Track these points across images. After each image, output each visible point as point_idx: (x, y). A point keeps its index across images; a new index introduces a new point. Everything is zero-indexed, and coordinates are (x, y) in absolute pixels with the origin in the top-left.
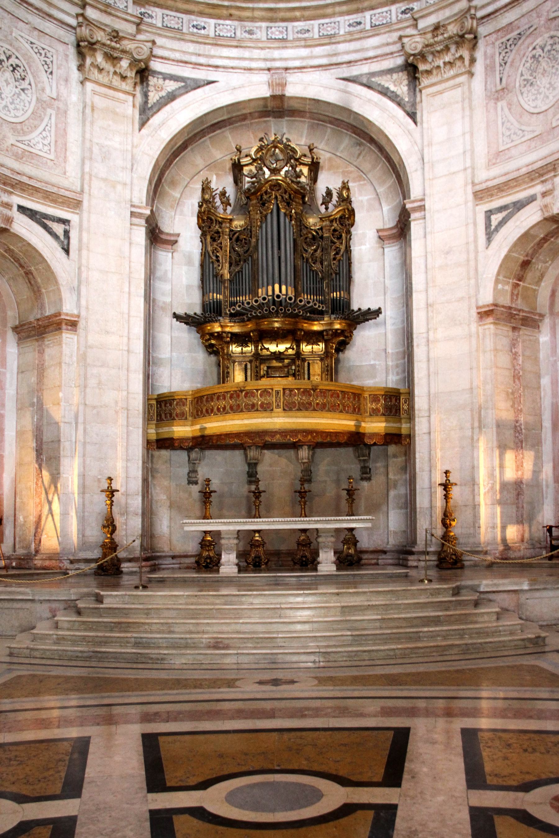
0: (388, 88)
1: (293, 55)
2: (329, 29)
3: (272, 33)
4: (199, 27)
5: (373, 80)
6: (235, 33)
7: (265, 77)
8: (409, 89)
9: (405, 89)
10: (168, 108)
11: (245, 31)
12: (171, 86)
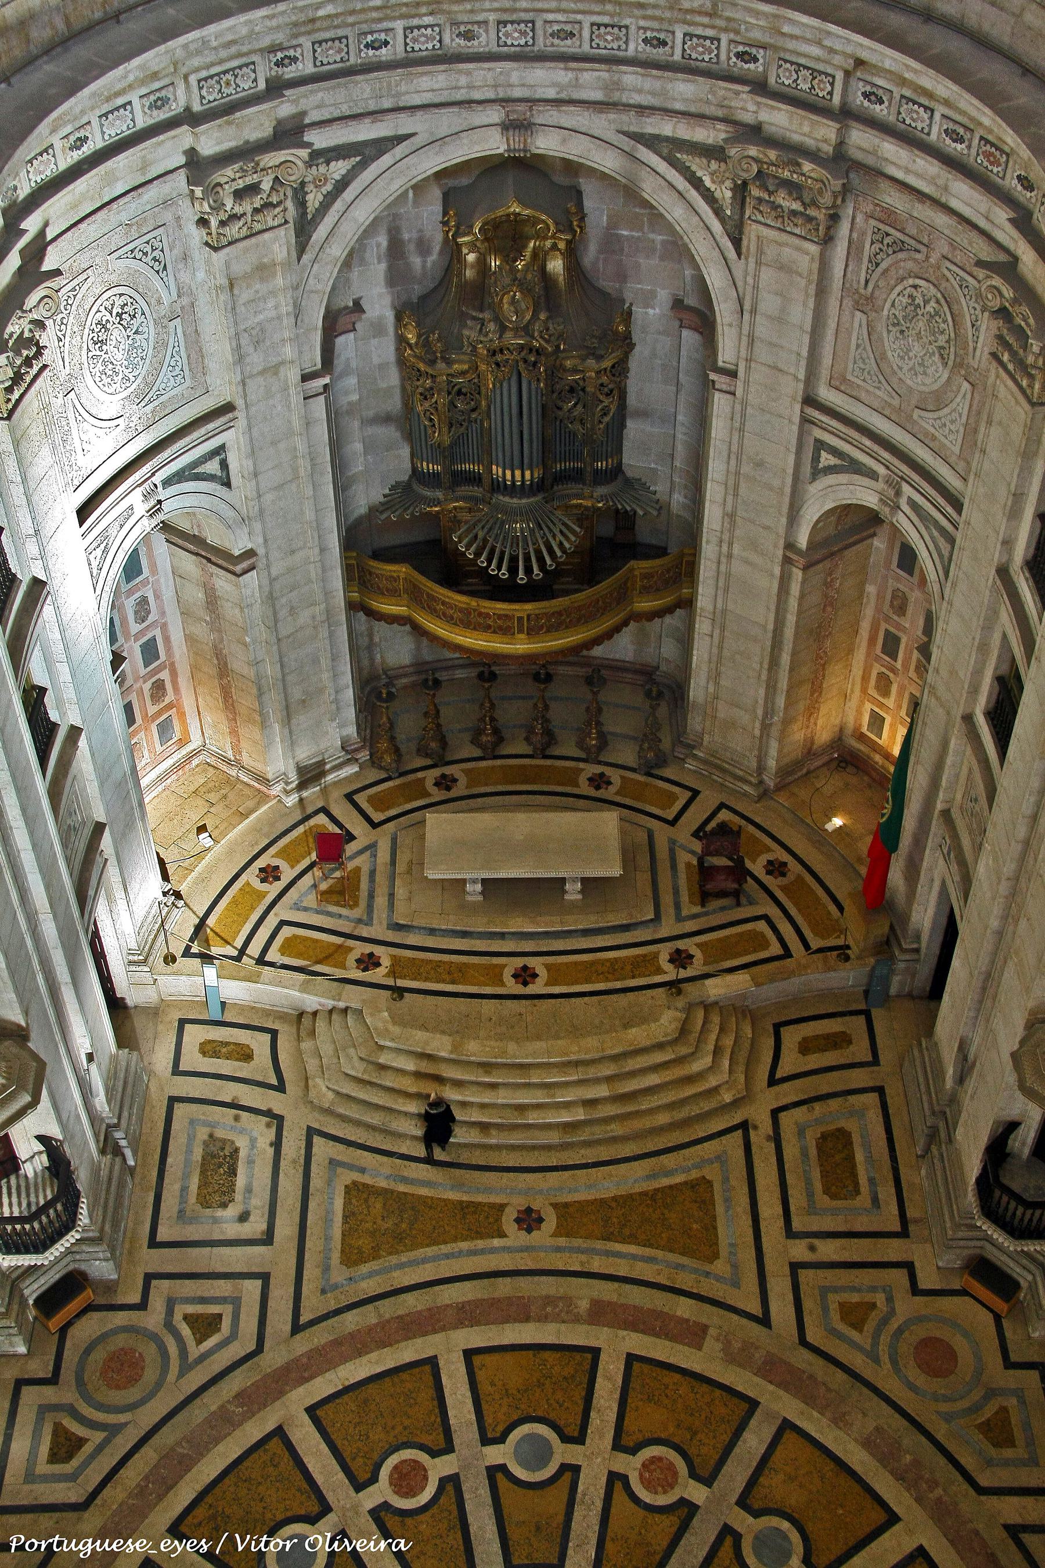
0: (700, 180)
1: (544, 80)
2: (609, 38)
3: (507, 35)
4: (376, 45)
5: (679, 155)
6: (440, 41)
7: (495, 115)
8: (733, 198)
9: (728, 194)
10: (338, 205)
11: (459, 35)
12: (339, 168)
